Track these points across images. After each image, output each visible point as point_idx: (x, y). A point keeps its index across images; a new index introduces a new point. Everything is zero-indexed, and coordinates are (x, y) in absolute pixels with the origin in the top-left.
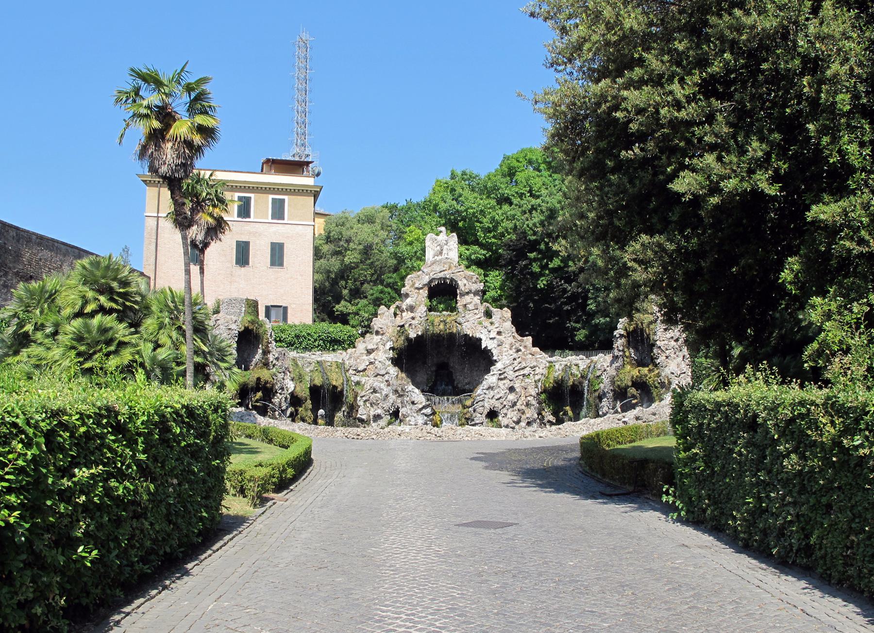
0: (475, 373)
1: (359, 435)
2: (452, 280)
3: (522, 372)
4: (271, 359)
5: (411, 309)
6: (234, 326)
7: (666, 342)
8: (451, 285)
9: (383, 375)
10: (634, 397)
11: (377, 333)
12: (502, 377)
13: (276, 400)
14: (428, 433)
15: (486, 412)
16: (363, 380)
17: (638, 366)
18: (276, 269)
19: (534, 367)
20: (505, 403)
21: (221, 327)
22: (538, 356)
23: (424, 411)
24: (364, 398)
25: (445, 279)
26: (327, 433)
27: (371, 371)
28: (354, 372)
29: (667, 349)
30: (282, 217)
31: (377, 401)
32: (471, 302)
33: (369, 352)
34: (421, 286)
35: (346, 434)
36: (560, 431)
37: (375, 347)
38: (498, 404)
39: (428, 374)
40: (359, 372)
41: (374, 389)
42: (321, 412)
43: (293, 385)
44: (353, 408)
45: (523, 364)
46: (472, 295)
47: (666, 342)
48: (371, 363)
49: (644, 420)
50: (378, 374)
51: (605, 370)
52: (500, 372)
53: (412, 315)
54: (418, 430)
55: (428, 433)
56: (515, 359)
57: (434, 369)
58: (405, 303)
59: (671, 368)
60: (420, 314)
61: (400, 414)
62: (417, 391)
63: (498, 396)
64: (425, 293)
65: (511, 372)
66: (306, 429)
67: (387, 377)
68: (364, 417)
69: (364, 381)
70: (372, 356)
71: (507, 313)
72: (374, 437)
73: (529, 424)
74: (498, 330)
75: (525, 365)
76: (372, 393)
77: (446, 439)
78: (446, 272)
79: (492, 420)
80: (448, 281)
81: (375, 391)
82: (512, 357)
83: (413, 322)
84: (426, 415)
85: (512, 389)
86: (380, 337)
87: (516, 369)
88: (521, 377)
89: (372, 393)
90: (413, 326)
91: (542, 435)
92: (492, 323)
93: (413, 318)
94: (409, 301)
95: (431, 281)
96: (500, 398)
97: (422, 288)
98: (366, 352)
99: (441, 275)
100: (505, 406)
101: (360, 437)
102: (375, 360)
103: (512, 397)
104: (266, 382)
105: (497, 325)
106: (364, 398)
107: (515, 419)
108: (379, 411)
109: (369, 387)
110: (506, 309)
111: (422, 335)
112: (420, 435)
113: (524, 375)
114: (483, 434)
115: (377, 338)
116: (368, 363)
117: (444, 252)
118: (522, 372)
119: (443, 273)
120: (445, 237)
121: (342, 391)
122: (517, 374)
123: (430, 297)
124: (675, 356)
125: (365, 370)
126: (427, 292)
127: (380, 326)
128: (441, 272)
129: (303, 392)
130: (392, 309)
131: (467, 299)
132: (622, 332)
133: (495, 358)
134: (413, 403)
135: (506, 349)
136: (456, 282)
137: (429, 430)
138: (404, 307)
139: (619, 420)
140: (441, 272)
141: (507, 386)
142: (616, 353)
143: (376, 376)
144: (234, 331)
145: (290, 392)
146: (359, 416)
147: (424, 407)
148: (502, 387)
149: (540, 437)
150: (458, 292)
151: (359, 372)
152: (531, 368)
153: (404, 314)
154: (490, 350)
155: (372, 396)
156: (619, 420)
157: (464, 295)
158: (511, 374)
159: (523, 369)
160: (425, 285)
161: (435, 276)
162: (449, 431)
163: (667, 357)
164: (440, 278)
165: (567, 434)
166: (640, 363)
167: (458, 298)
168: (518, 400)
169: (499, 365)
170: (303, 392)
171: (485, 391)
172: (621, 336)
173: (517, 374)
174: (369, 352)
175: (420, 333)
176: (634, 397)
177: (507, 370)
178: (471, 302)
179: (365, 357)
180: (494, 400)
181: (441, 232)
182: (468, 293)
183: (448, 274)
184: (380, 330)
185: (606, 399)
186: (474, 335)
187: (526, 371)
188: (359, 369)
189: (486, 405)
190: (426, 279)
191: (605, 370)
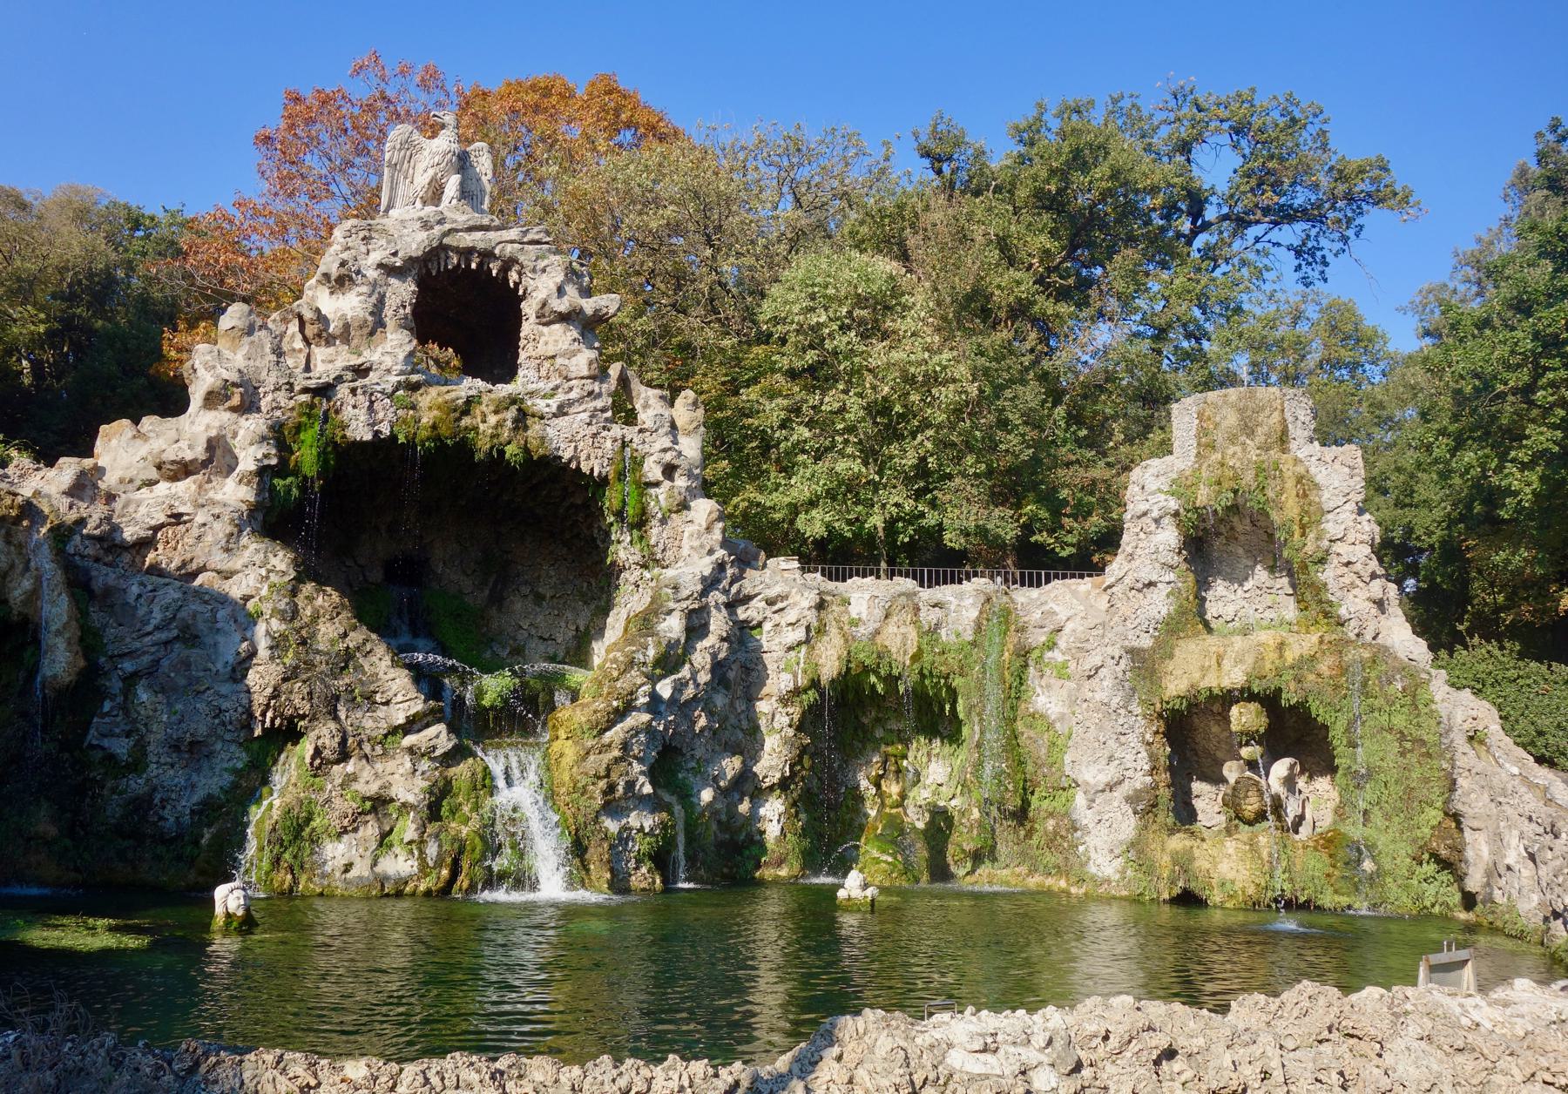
25: (487, 255)
32: (574, 354)
60: (388, 361)
69: (135, 589)
74: (668, 457)
78: (492, 235)
95: (438, 252)
98: (153, 474)
109: (157, 617)
119: (478, 235)
126: (414, 287)
147: (413, 724)
152: (770, 602)
160: (411, 260)
164: (467, 252)
186: (585, 468)
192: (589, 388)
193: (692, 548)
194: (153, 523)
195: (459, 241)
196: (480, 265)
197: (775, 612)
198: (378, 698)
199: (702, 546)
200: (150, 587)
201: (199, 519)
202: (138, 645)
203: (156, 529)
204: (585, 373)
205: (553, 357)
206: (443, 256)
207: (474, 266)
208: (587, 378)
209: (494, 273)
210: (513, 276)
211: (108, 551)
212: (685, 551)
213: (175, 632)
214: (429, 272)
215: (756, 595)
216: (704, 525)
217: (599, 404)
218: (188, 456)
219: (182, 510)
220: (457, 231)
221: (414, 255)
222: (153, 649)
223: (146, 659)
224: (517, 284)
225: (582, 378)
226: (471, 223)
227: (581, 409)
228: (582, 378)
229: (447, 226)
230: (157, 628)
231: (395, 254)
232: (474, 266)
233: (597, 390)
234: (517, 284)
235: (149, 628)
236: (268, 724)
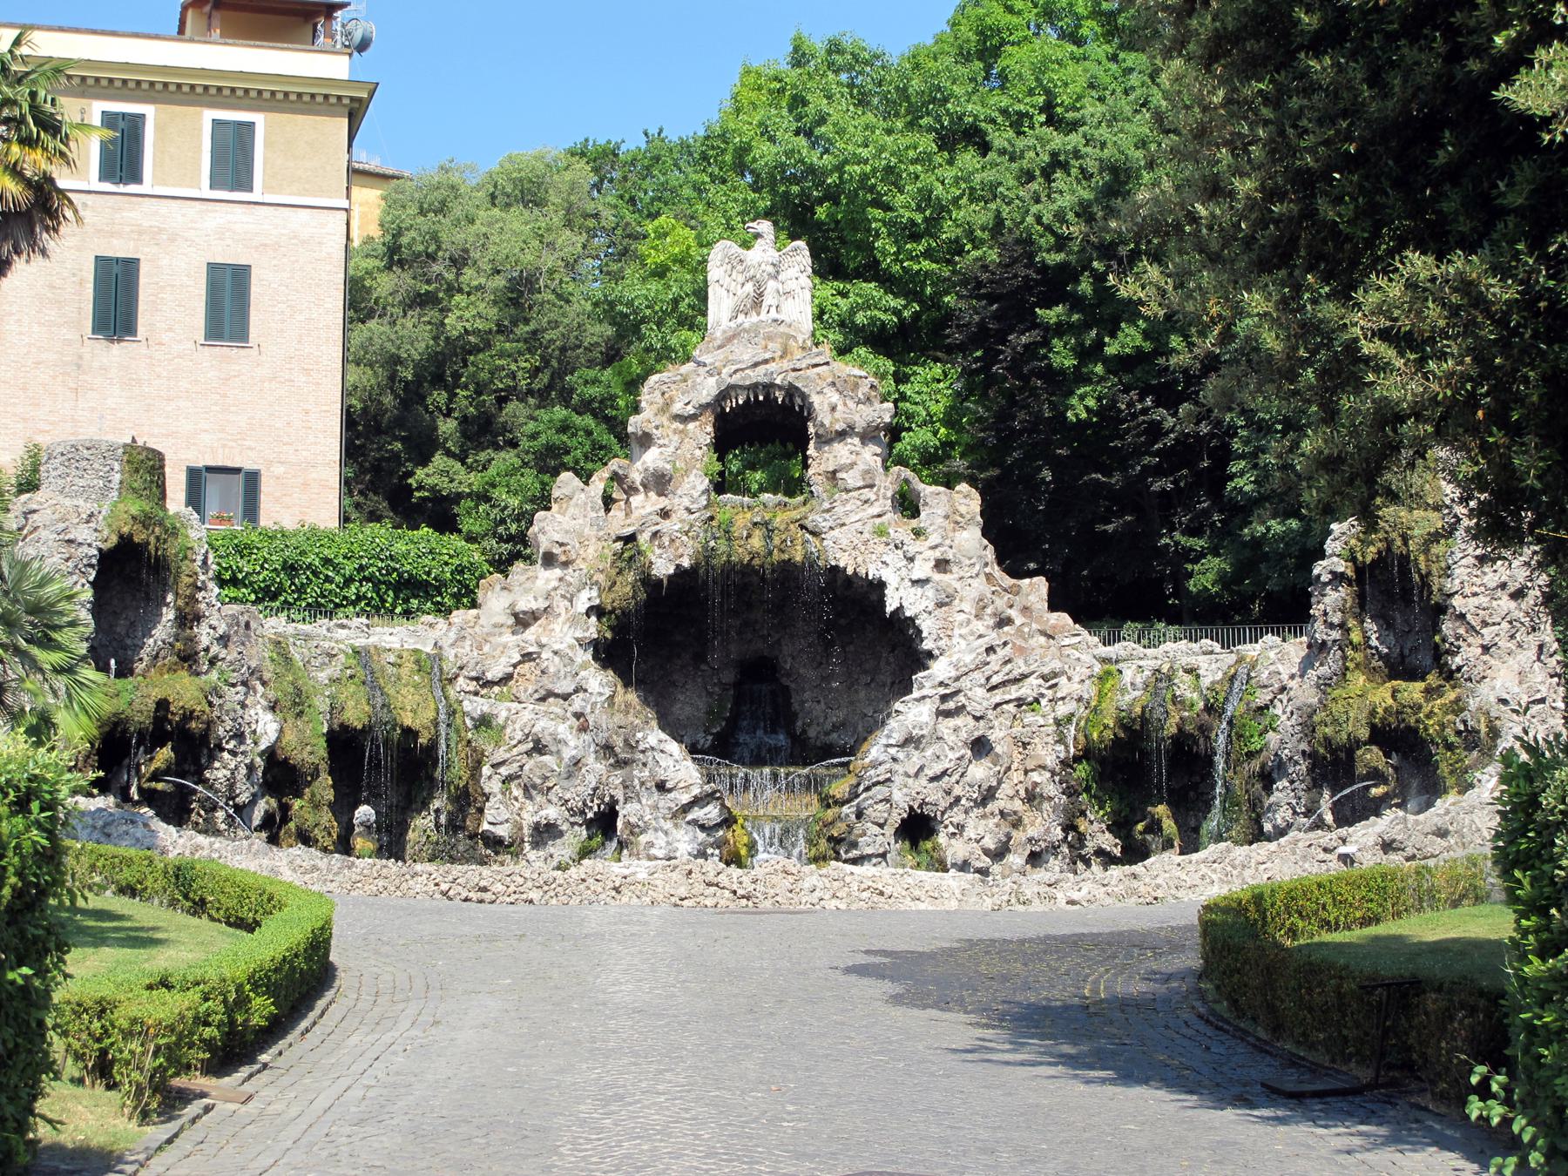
0: (862, 694)
1: (484, 889)
2: (791, 391)
3: (1014, 692)
4: (205, 641)
5: (660, 482)
6: (83, 533)
7: (1483, 600)
8: (787, 408)
9: (566, 697)
10: (1377, 776)
11: (549, 560)
12: (951, 705)
13: (218, 773)
14: (709, 884)
15: (896, 819)
16: (502, 711)
17: (1391, 677)
18: (224, 352)
19: (1055, 675)
20: (957, 791)
21: (43, 534)
22: (1067, 642)
23: (696, 813)
24: (504, 771)
25: (769, 387)
26: (381, 883)
27: (525, 686)
28: (473, 686)
29: (1485, 624)
30: (135, 176)
31: (546, 778)
32: (852, 465)
33: (523, 621)
34: (690, 410)
35: (444, 887)
36: (1135, 884)
37: (542, 604)
38: (934, 795)
39: (710, 694)
40: (489, 684)
41: (537, 741)
42: (364, 812)
43: (275, 726)
44: (467, 800)
45: (1019, 667)
46: (856, 440)
47: (1483, 600)
48: (527, 657)
49: (1410, 851)
50: (550, 694)
51: (1283, 689)
52: (942, 691)
53: (663, 502)
54: (674, 875)
55: (709, 884)
56: (990, 650)
57: (729, 676)
58: (638, 465)
59: (1498, 683)
60: (686, 502)
61: (620, 824)
62: (674, 747)
63: (937, 768)
64: (703, 431)
65: (980, 692)
66: (315, 868)
67: (577, 703)
68: (502, 831)
69: (504, 714)
70: (531, 633)
71: (968, 500)
72: (535, 895)
73: (1035, 859)
74: (937, 554)
75: (1024, 669)
76: (529, 753)
77: (767, 904)
78: (772, 367)
79: (914, 845)
80: (780, 396)
81: (539, 748)
82: (983, 643)
83: (665, 526)
84: (702, 827)
85: (980, 747)
86: (558, 572)
87: (995, 680)
88: (1011, 707)
89: (529, 753)
90: (666, 540)
91: (1076, 896)
92: (918, 533)
93: (665, 514)
94: (652, 458)
95: (723, 395)
96: (944, 773)
97: (693, 417)
99: (758, 376)
100: (958, 799)
101: (488, 896)
102: (542, 646)
103: (980, 771)
104: (189, 716)
105: (934, 539)
106: (504, 771)
107: (989, 842)
108: (552, 813)
109: (519, 736)
110: (963, 487)
111: (694, 569)
112: (682, 892)
113: (1020, 702)
114: (888, 891)
115: (547, 578)
116: (517, 658)
117: (769, 299)
118: (1014, 692)
119: (761, 369)
120: (773, 255)
121: (433, 746)
122: (998, 696)
123: (722, 445)
124: (1512, 645)
125: (507, 678)
126: (710, 429)
127: (557, 537)
128: (756, 365)
129: (308, 747)
130: (598, 484)
131: (841, 453)
132: (1341, 566)
133: (927, 645)
134: (661, 787)
135: (962, 617)
136: (804, 397)
137: (711, 877)
138: (636, 477)
139: (1326, 850)
140: (756, 365)
141: (963, 735)
142: (1320, 632)
143: (543, 699)
144: (85, 549)
145: (262, 747)
146: (485, 826)
147: (697, 802)
148: (951, 738)
149: (1071, 902)
150: (811, 430)
151: (489, 684)
152: (1045, 678)
153: (636, 500)
154: (912, 620)
155: (530, 764)
156: (1326, 850)
157: (829, 442)
158: (977, 697)
159: (1016, 681)
160: (703, 407)
161: (735, 380)
162: (775, 879)
163: (1486, 649)
164: (754, 387)
165: (1159, 894)
166: (1399, 668)
167: (811, 451)
168: (1000, 782)
169: (940, 669)
170: (308, 747)
171: (893, 751)
172: (1338, 578)
173: (998, 699)
174: (523, 621)
175: (686, 563)
176: (1377, 776)
177: (965, 683)
178: (852, 465)
179: (508, 638)
180: (923, 781)
181: (757, 236)
182: (841, 435)
183: (778, 373)
184: (557, 550)
185: (1284, 783)
186: (862, 572)
187: (1027, 690)
188: (489, 676)
189: (898, 796)
190: (708, 389)
191: (1283, 689)
192: (863, 498)
193: (961, 635)
194: (514, 661)
195: (743, 379)
196: (767, 397)
197: (1050, 688)
198: (669, 785)
199: (972, 633)
200: (514, 711)
201: (544, 656)
202: (508, 755)
203: (515, 666)
204: (861, 484)
205: (834, 472)
206: (733, 394)
207: (761, 398)
208: (864, 487)
209: (780, 400)
210: (798, 401)
211: (483, 686)
212: (955, 640)
213: (531, 745)
214: (723, 409)
215: (1034, 672)
216: (973, 612)
217: (875, 510)
218: (534, 605)
219: (531, 649)
220: (742, 370)
221: (704, 401)
223: (516, 765)
224: (801, 408)
225: (859, 488)
226: (756, 359)
227: (857, 518)
228: (859, 488)
229: (734, 368)
230: (520, 742)
231: (687, 404)
232: (761, 398)
233: (873, 497)
234: (801, 408)
235: (514, 742)
236: (596, 809)
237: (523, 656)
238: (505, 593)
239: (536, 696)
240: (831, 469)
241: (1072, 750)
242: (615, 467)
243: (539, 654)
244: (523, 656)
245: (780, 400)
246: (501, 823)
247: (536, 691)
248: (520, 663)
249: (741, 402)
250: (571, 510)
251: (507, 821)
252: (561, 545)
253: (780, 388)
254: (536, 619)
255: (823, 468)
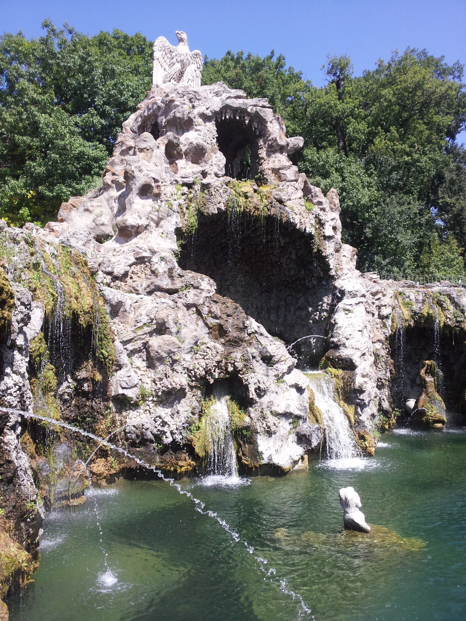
16: (129, 299)
24: (130, 347)
28: (108, 279)
31: (170, 353)
40: (115, 278)
48: (140, 260)
50: (159, 289)
79: (129, 357)
89: (151, 334)
102: (154, 252)
109: (145, 319)
111: (225, 212)
116: (133, 260)
121: (90, 326)
125: (126, 274)
133: (333, 273)
154: (326, 257)
157: (274, 152)
204: (293, 178)
205: (280, 169)
209: (247, 122)
213: (155, 327)
219: (145, 254)
222: (143, 337)
225: (292, 181)
228: (292, 181)
231: (207, 109)
232: (238, 118)
237: (137, 259)
238: (87, 213)
239: (148, 290)
240: (277, 167)
241: (390, 332)
242: (171, 138)
243: (150, 258)
244: (137, 259)
245: (247, 122)
246: (132, 387)
247: (148, 286)
248: (134, 264)
249: (227, 117)
250: (154, 159)
251: (135, 386)
252: (156, 181)
253: (249, 114)
254: (137, 233)
255: (271, 165)
